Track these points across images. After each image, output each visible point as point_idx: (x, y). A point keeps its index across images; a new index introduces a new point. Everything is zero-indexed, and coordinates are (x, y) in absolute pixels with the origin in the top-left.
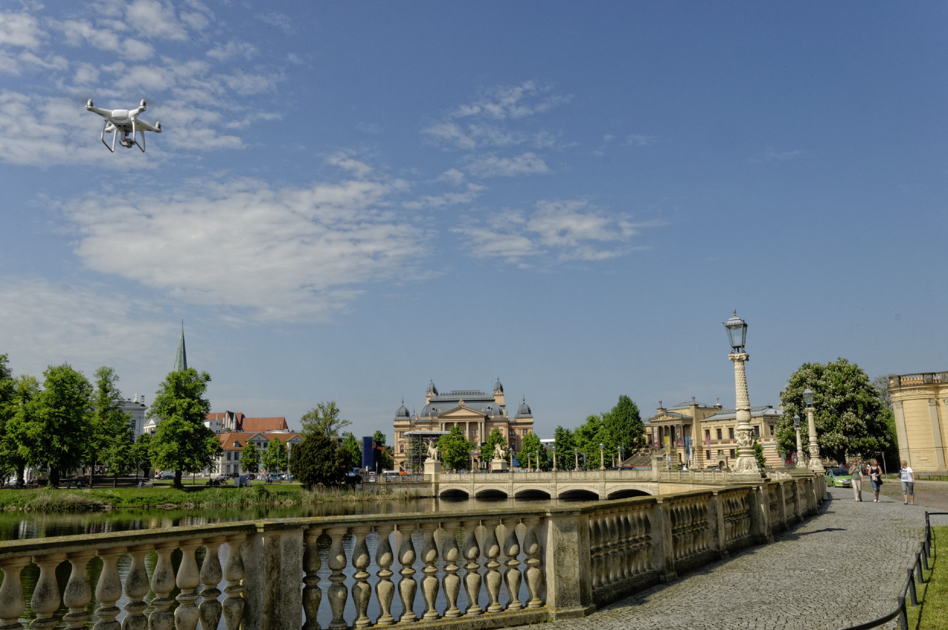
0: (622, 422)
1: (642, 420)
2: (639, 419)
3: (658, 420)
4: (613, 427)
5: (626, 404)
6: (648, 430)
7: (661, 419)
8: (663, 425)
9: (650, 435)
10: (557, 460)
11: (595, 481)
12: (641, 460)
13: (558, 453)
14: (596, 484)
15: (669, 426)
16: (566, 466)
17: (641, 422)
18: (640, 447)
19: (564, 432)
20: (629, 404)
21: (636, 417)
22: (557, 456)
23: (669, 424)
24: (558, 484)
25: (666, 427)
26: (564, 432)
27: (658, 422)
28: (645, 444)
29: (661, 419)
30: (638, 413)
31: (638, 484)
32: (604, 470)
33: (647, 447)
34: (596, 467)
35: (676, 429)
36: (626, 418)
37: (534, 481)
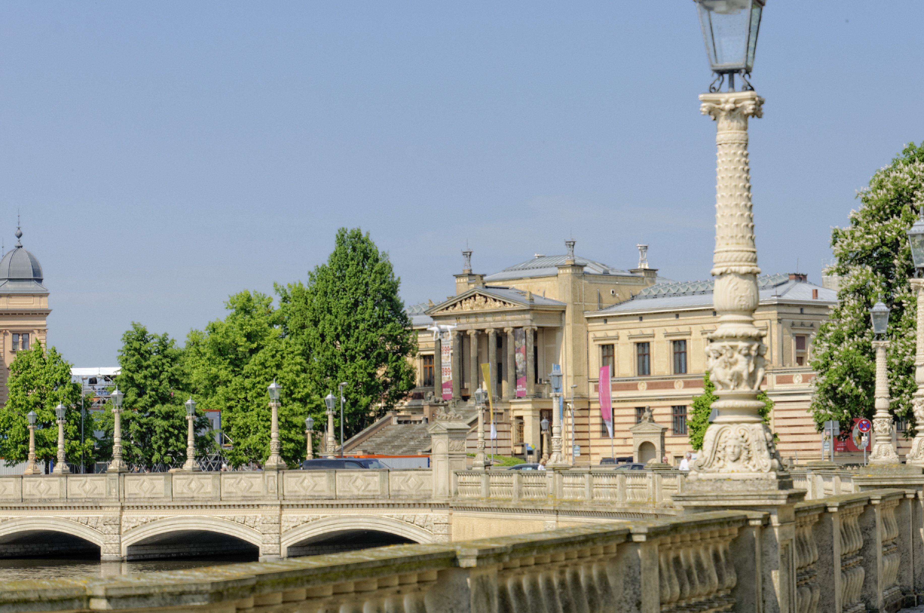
0: (342, 316)
1: (406, 309)
2: (396, 308)
3: (457, 310)
4: (311, 332)
5: (357, 255)
6: (425, 343)
7: (467, 307)
8: (471, 326)
9: (428, 358)
10: (125, 437)
11: (249, 503)
12: (396, 437)
13: (129, 414)
14: (250, 514)
15: (491, 332)
16: (156, 456)
17: (404, 318)
18: (400, 396)
19: (153, 345)
20: (366, 257)
21: (389, 298)
22: (125, 423)
23: (490, 325)
24: (127, 514)
25: (481, 334)
26: (153, 345)
27: (458, 317)
28: (412, 387)
29: (467, 307)
30: (394, 288)
31: (385, 513)
32: (279, 469)
33: (419, 396)
34: (256, 458)
35: (510, 340)
36: (356, 304)
37: (46, 505)
